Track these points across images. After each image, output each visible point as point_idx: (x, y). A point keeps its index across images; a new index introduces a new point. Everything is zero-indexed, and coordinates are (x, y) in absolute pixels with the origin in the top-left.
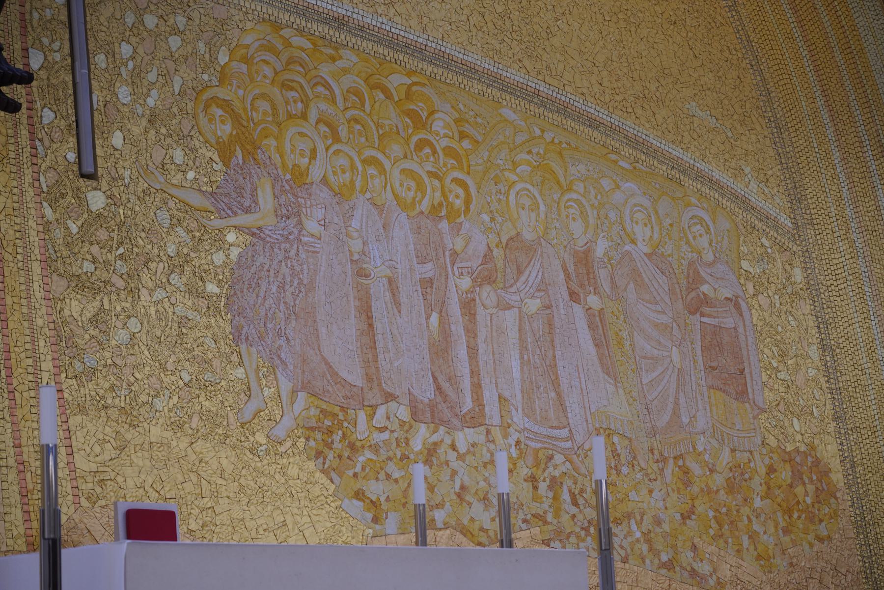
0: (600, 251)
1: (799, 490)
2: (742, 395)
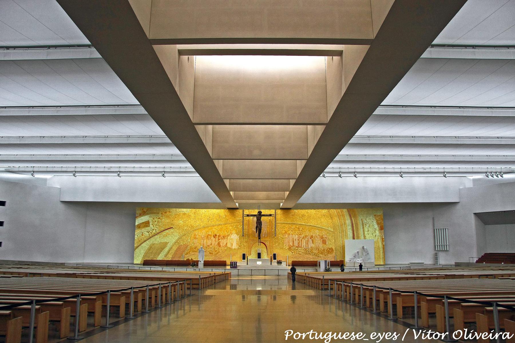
0: (313, 235)
1: (330, 251)
2: (326, 244)
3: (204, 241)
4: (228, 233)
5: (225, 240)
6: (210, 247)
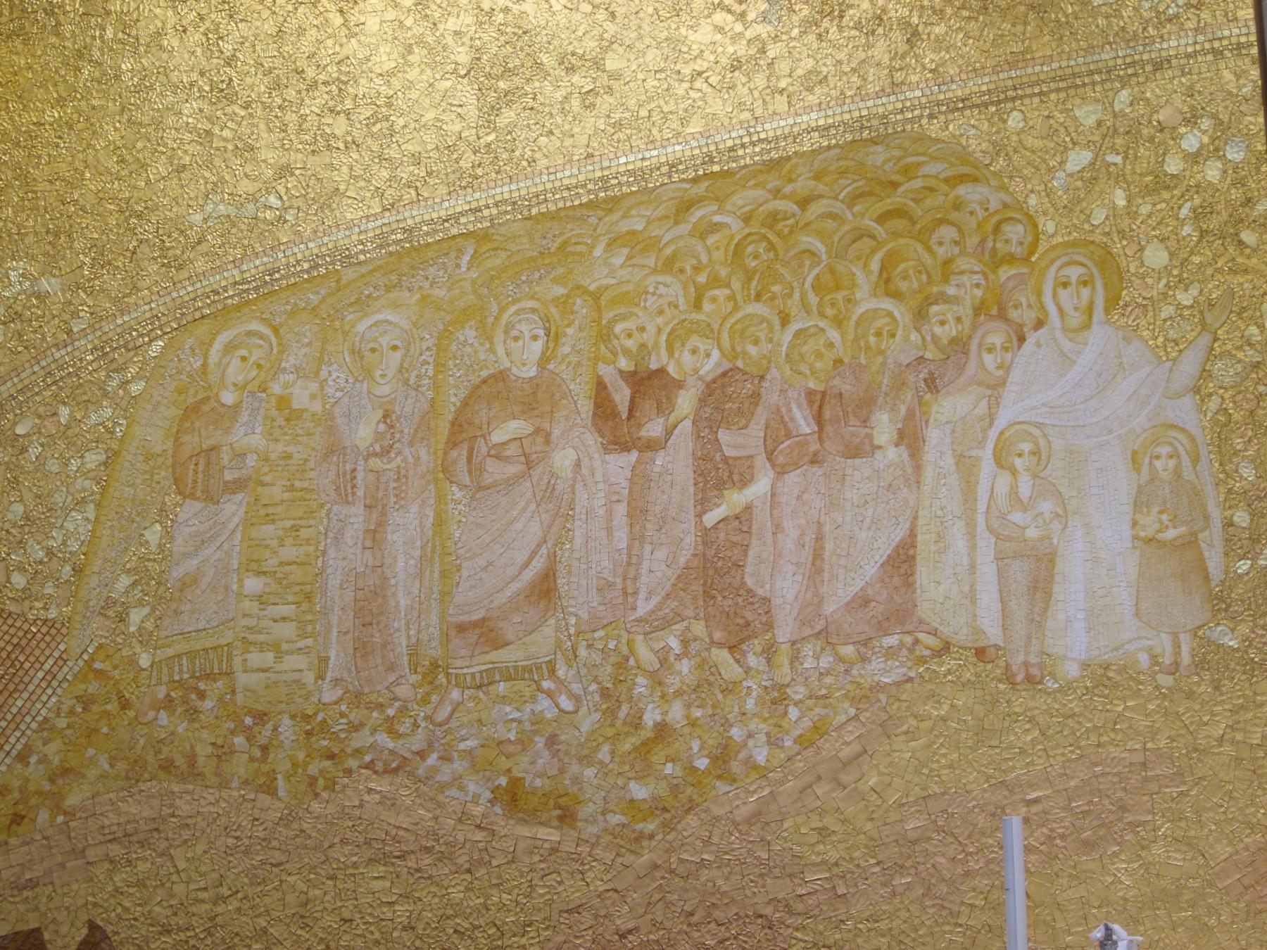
3: (375, 536)
4: (920, 315)
5: (859, 474)
6: (505, 656)
